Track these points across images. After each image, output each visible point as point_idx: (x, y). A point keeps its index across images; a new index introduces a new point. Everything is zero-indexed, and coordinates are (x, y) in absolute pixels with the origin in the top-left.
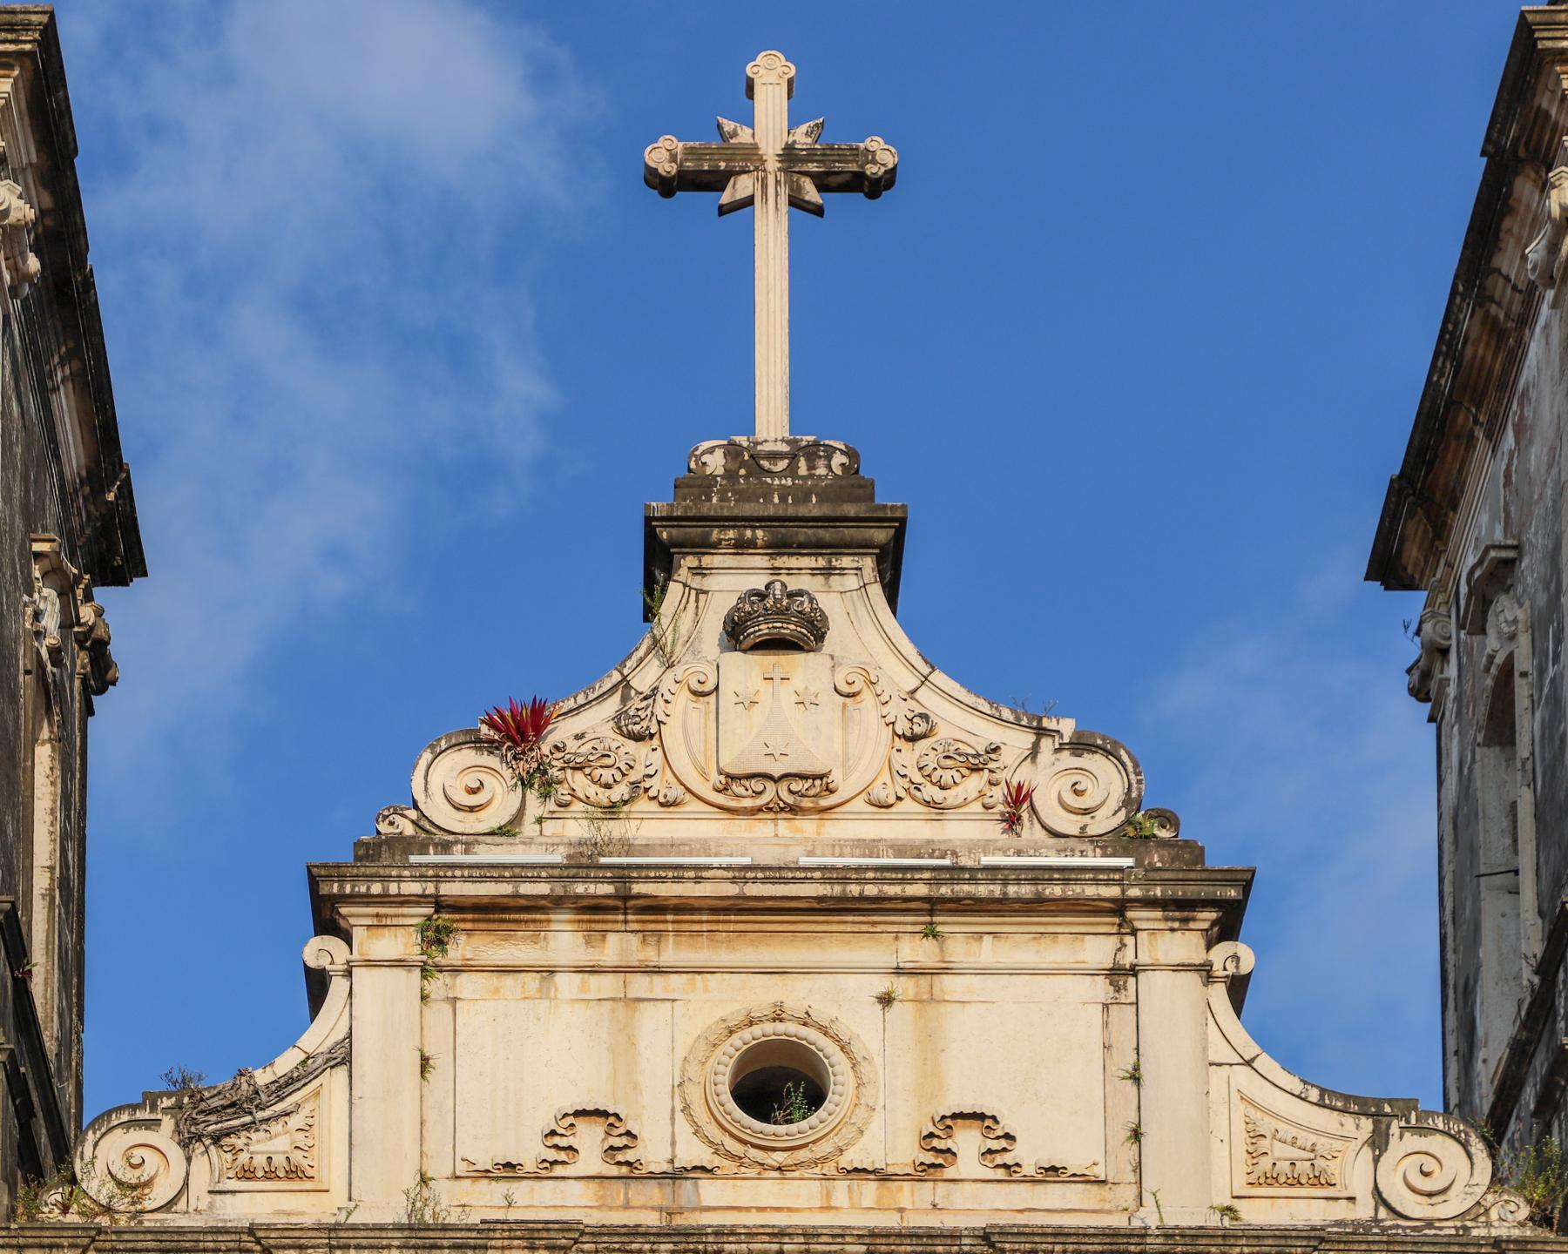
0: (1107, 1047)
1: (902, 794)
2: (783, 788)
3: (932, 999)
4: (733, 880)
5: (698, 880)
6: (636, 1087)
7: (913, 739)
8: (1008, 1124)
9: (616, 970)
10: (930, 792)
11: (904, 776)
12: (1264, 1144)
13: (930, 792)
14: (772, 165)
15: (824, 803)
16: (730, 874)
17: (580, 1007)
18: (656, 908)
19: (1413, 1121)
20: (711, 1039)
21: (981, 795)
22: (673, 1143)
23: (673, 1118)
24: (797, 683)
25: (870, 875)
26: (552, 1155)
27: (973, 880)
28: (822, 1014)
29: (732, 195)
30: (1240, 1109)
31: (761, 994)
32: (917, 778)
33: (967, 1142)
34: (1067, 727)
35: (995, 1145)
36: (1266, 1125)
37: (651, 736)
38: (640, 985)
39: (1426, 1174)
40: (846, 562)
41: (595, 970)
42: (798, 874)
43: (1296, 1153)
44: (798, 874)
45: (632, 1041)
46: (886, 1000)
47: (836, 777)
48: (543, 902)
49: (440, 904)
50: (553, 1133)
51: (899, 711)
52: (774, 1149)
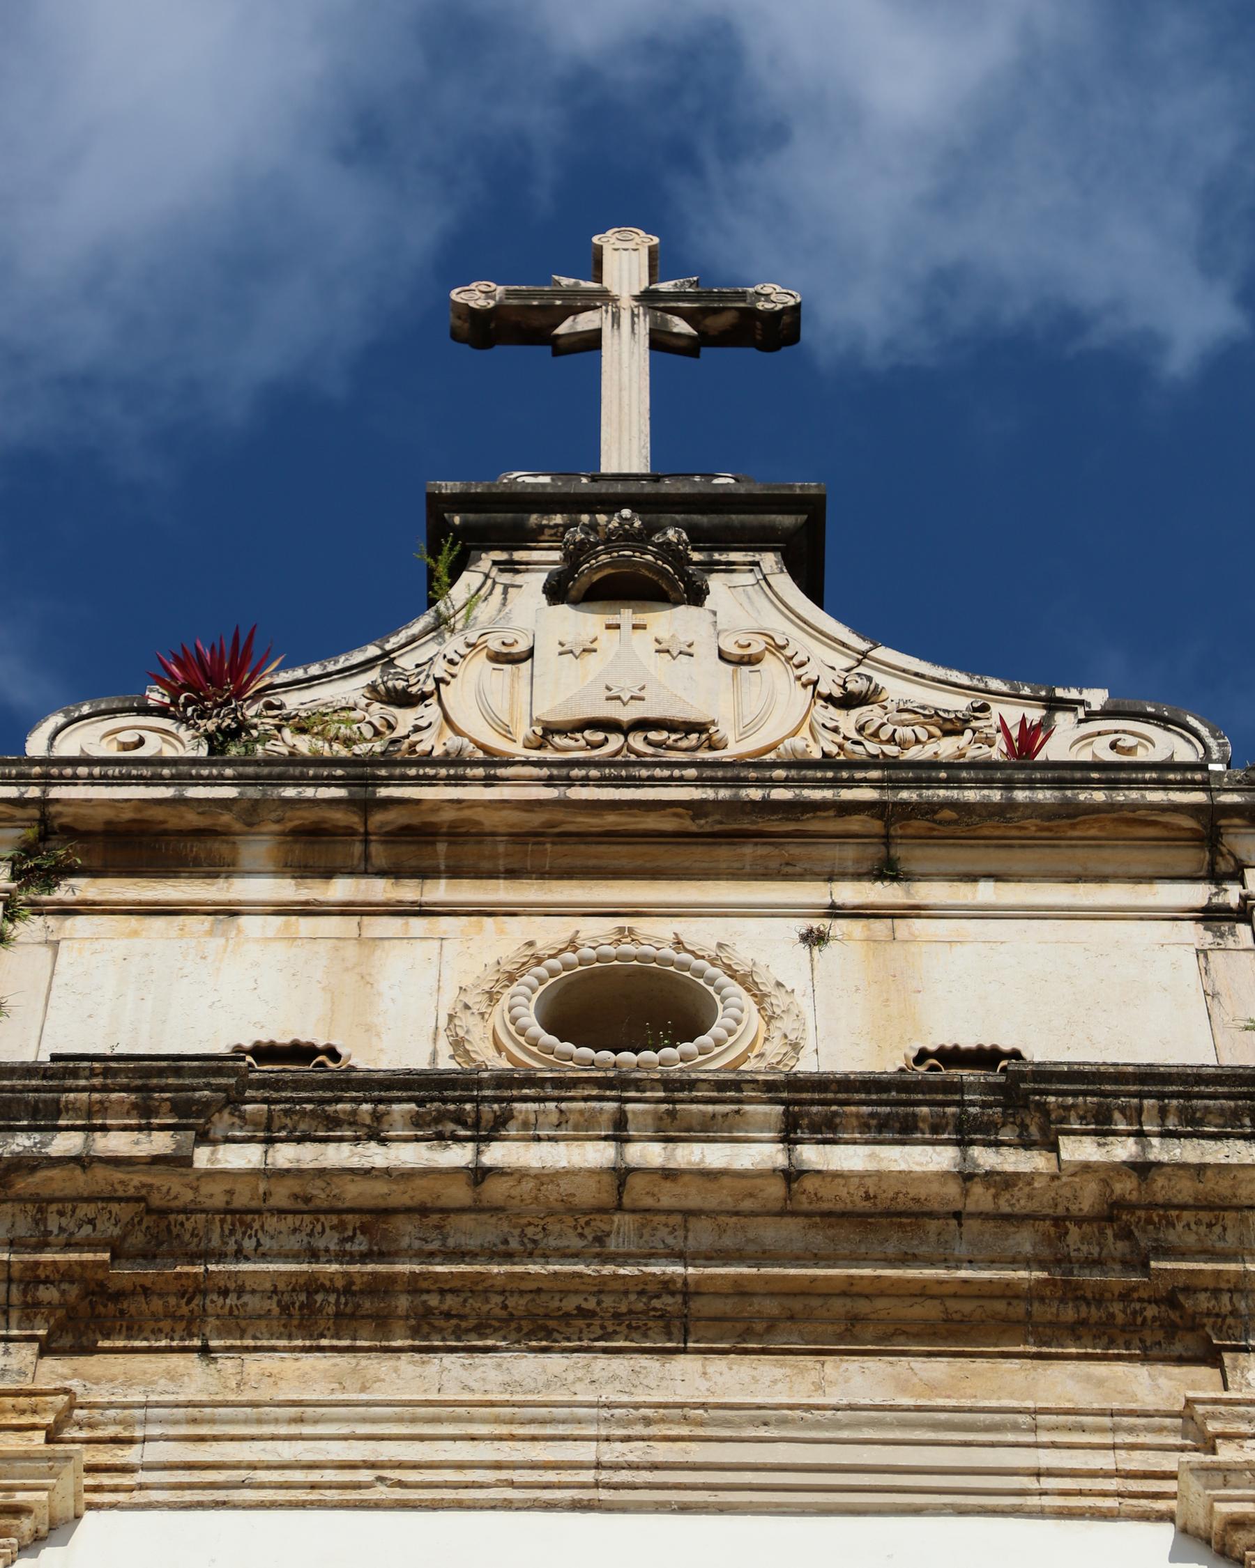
0: (1211, 995)
2: (637, 741)
4: (549, 782)
5: (489, 781)
7: (848, 701)
11: (835, 730)
14: (626, 303)
16: (545, 772)
20: (509, 968)
25: (780, 773)
27: (959, 784)
29: (571, 327)
34: (1097, 698)
37: (424, 697)
42: (658, 772)
44: (658, 772)
45: (366, 980)
48: (226, 818)
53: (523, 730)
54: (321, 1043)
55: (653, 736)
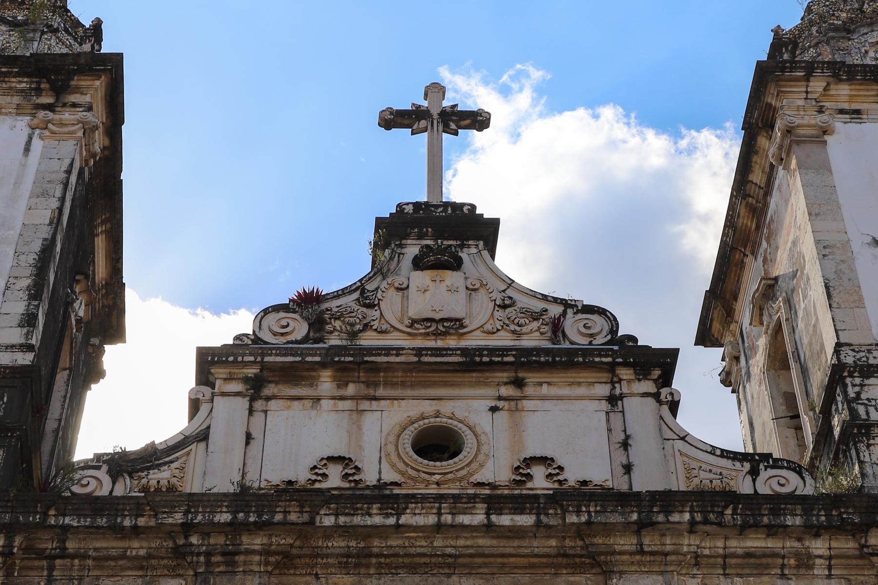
1: (500, 328)
3: (517, 410)
4: (415, 355)
5: (397, 355)
6: (361, 447)
7: (504, 307)
8: (560, 462)
9: (352, 398)
10: (512, 327)
12: (695, 473)
13: (512, 327)
15: (461, 331)
17: (333, 414)
18: (375, 368)
19: (771, 462)
21: (539, 328)
22: (380, 473)
23: (380, 462)
24: (448, 282)
26: (314, 477)
28: (459, 414)
30: (679, 459)
31: (428, 407)
32: (507, 322)
33: (539, 473)
35: (553, 472)
36: (695, 465)
38: (365, 405)
39: (782, 485)
40: (471, 242)
41: (342, 398)
43: (712, 476)
45: (359, 428)
46: (494, 409)
47: (466, 322)
49: (263, 366)
50: (315, 467)
51: (498, 297)
52: (434, 474)
53: (407, 322)
54: (347, 457)
55: (445, 324)
